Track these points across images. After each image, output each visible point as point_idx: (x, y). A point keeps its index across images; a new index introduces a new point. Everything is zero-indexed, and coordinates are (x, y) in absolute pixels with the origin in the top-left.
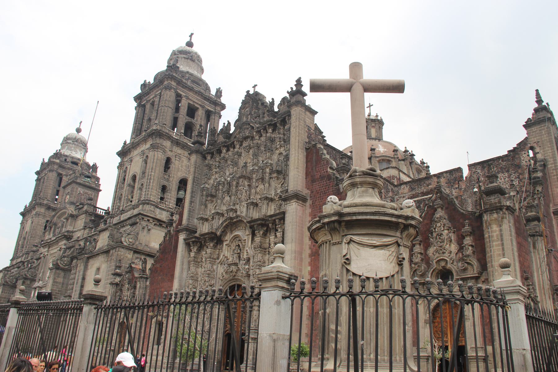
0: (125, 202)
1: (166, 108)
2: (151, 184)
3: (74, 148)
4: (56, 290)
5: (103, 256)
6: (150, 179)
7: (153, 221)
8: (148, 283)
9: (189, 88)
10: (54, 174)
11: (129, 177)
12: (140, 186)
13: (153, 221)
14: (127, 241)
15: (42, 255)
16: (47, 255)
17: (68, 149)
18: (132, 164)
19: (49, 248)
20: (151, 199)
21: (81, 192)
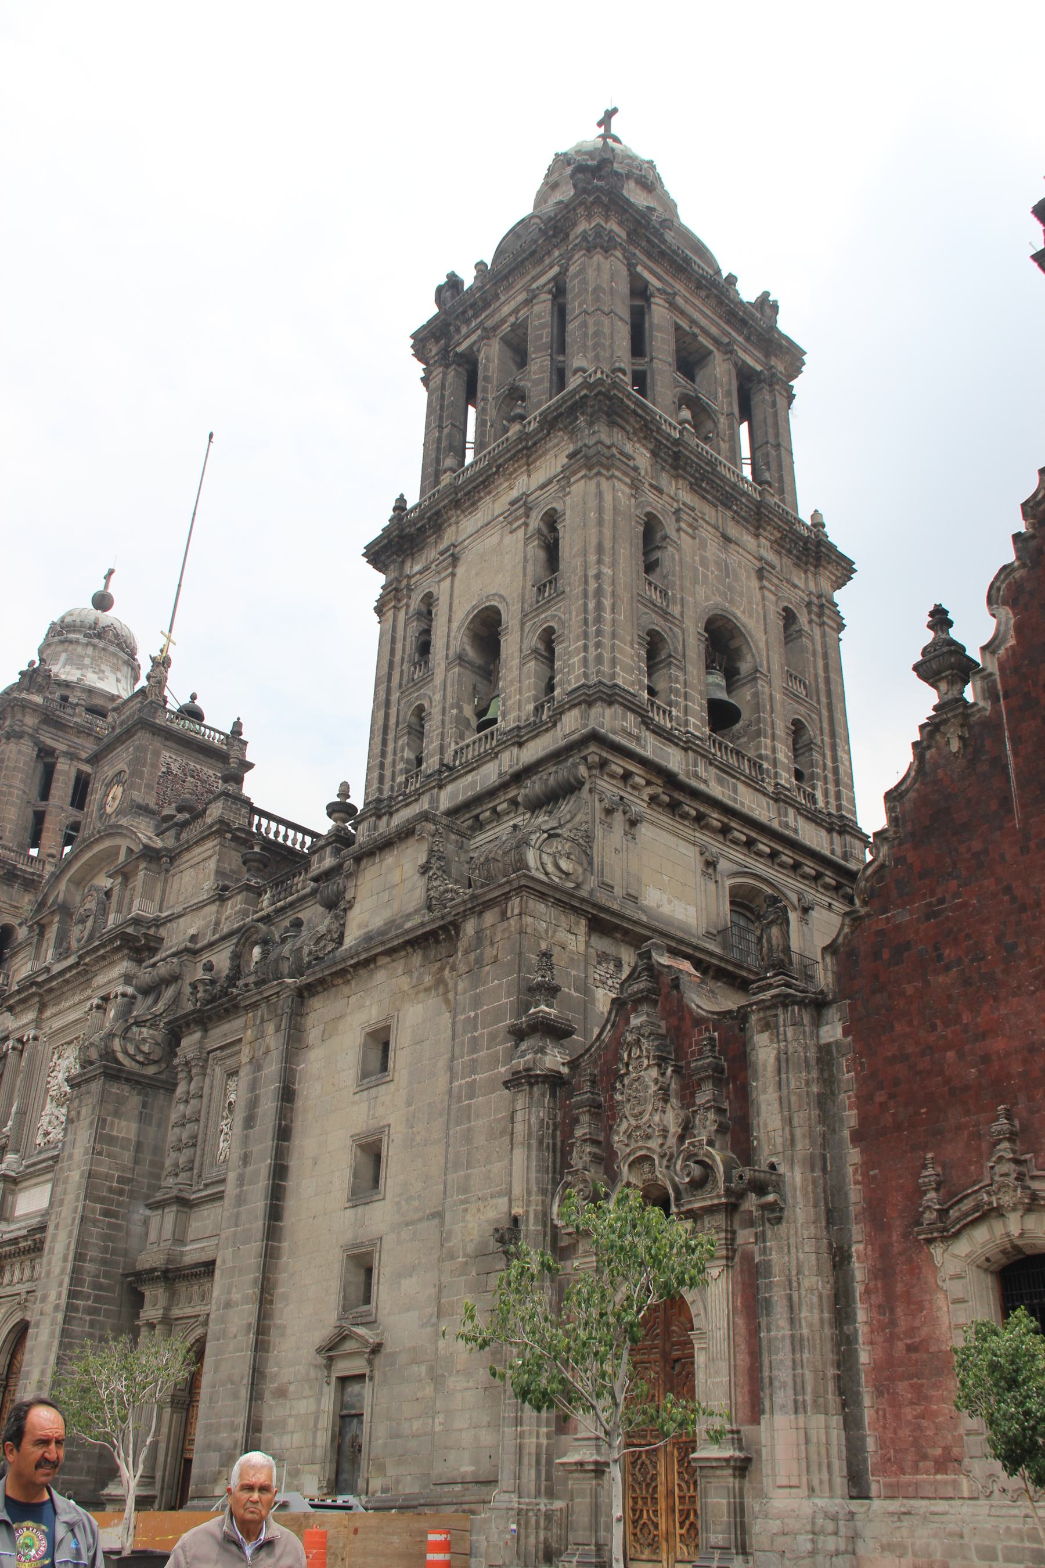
0: (451, 731)
1: (606, 321)
2: (607, 616)
3: (93, 659)
4: (108, 1177)
5: (399, 966)
6: (599, 592)
7: (649, 783)
8: (832, 1031)
9: (672, 262)
10: (24, 748)
11: (455, 625)
12: (533, 640)
13: (649, 783)
14: (550, 868)
15: (10, 1043)
16: (35, 1038)
17: (69, 662)
18: (460, 571)
19: (41, 1011)
20: (619, 681)
21: (175, 768)
